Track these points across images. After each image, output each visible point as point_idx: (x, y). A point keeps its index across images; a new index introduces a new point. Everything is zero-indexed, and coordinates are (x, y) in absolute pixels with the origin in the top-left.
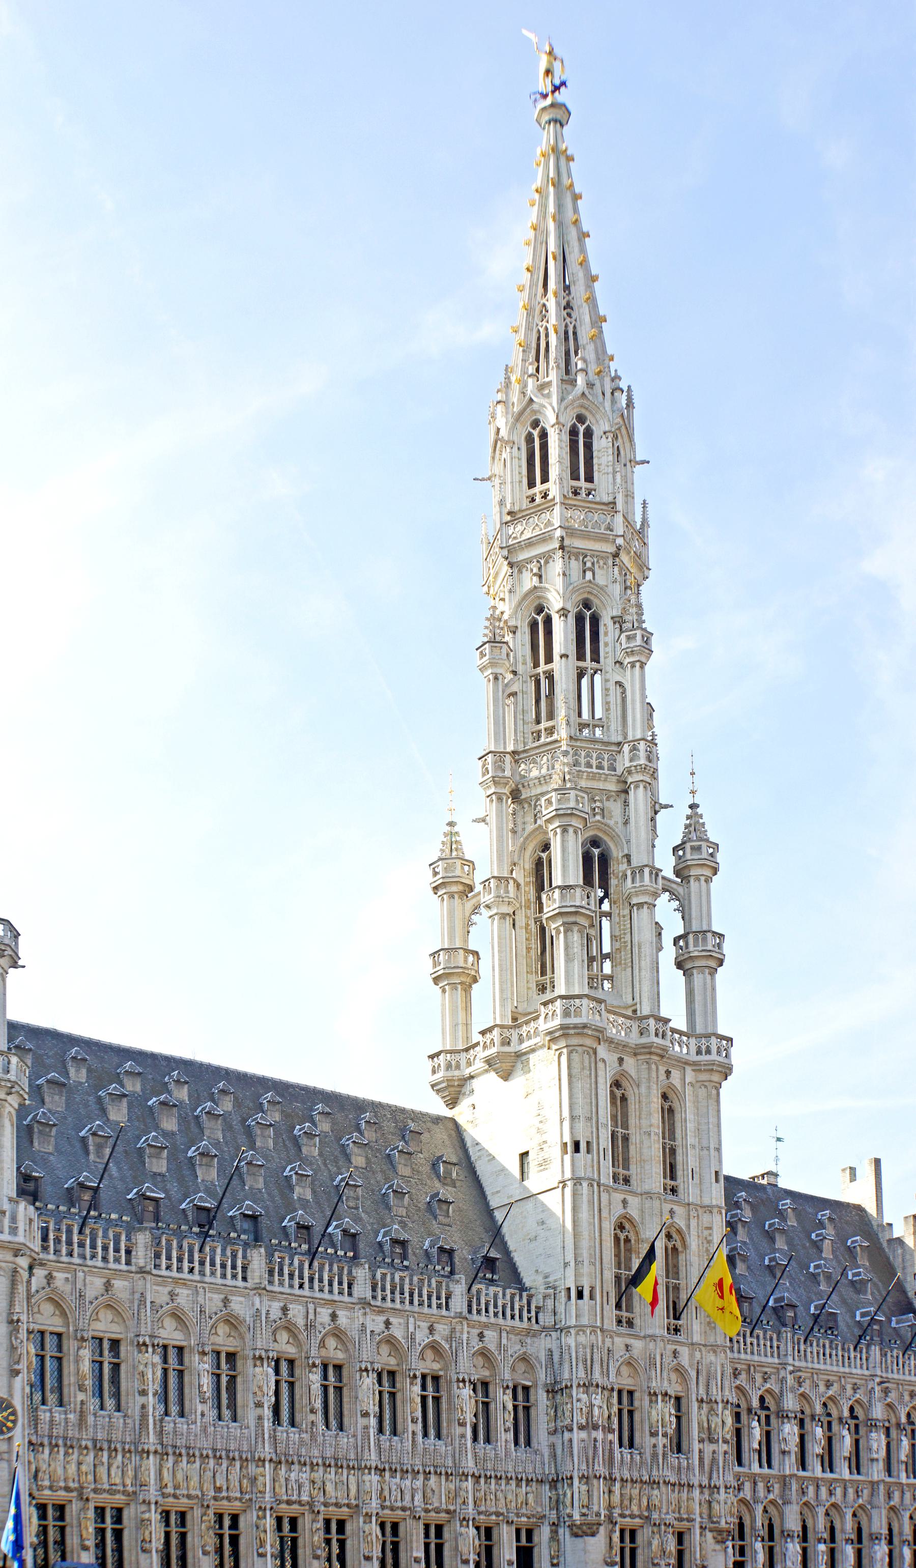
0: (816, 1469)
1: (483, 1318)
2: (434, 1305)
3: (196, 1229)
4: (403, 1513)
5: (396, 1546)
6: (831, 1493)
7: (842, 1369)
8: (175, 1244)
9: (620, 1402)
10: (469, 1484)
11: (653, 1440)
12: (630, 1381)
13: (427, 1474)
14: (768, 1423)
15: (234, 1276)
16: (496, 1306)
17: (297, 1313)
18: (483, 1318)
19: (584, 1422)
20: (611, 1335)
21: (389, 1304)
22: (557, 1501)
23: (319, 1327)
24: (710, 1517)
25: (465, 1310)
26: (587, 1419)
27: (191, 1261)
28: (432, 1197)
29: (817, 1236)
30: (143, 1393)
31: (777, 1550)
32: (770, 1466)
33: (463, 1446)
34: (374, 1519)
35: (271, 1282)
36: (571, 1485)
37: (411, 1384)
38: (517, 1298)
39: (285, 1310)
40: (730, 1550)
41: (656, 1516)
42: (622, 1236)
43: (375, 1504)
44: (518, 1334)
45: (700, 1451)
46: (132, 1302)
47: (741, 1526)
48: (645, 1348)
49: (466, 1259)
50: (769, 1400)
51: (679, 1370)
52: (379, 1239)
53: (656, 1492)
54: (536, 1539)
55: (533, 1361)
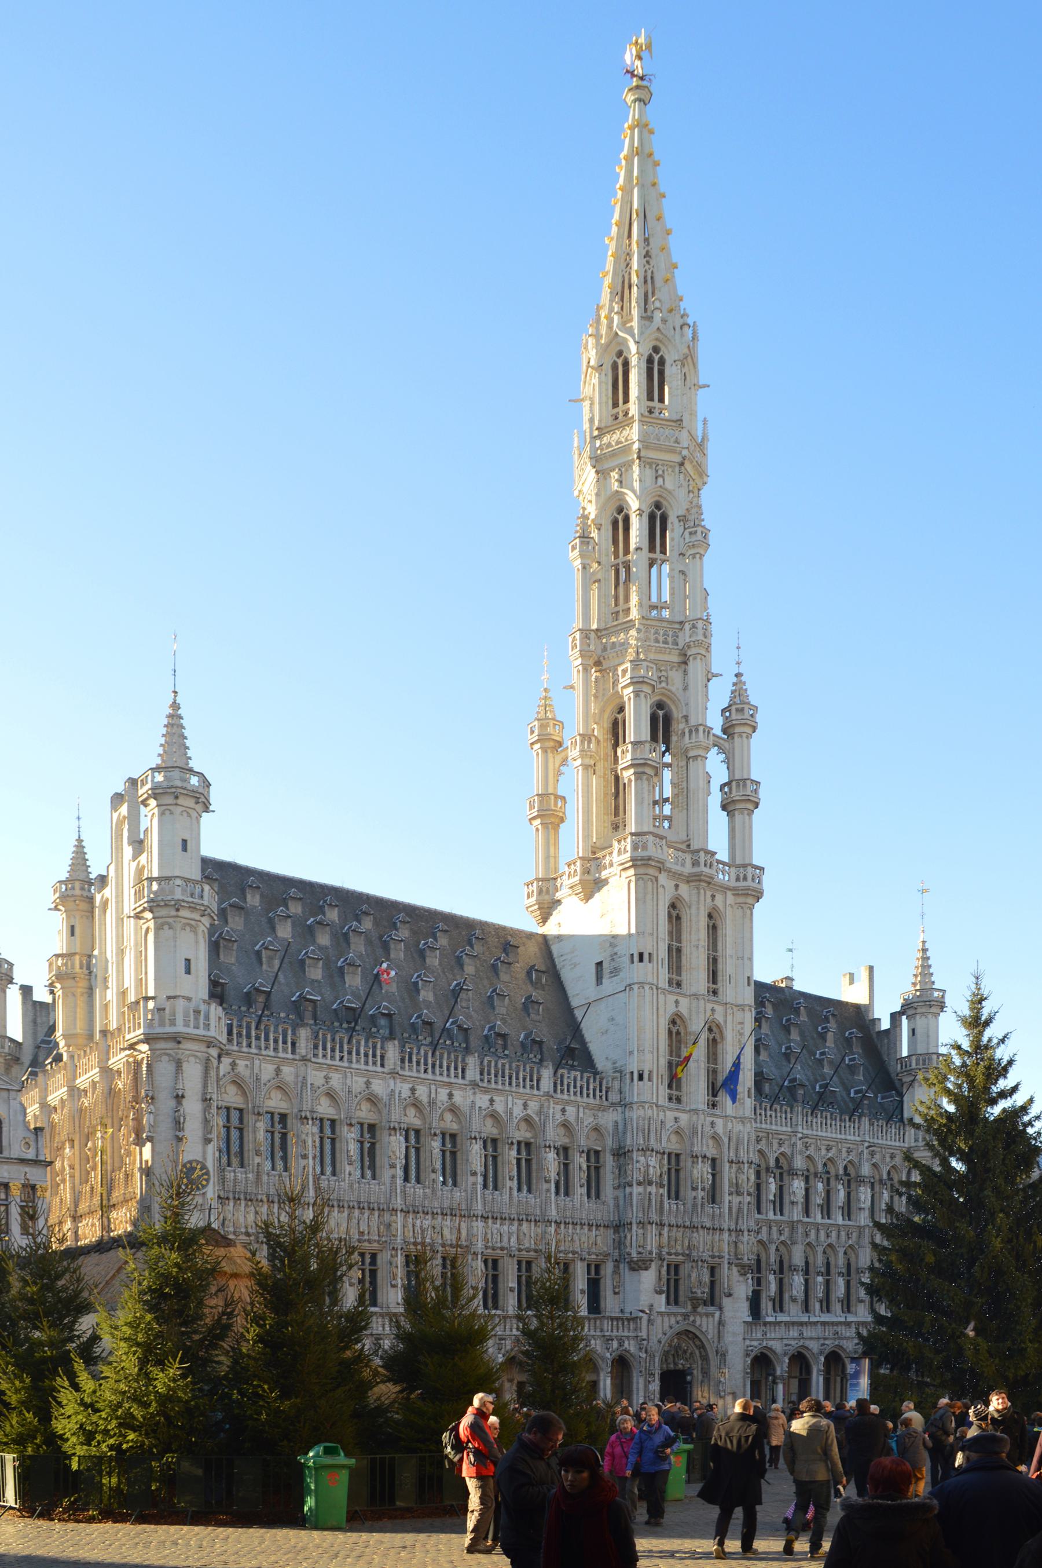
0: (818, 1217)
1: (565, 1097)
2: (528, 1086)
3: (345, 1025)
5: (495, 1278)
6: (828, 1236)
7: (839, 1136)
8: (329, 1037)
9: (669, 1163)
10: (552, 1229)
11: (694, 1193)
12: (678, 1146)
13: (520, 1221)
14: (781, 1180)
15: (374, 1063)
16: (575, 1087)
17: (422, 1092)
18: (565, 1097)
19: (641, 1179)
21: (493, 1086)
22: (619, 1242)
23: (439, 1104)
24: (736, 1254)
25: (552, 1090)
27: (341, 1051)
28: (526, 999)
29: (823, 1028)
30: (305, 1157)
31: (786, 1281)
32: (782, 1214)
33: (548, 1200)
35: (402, 1068)
36: (630, 1230)
37: (510, 1149)
38: (592, 1080)
39: (413, 1090)
40: (750, 1281)
42: (674, 1030)
43: (480, 1246)
45: (730, 1202)
46: (296, 1084)
47: (759, 1261)
48: (690, 1120)
49: (552, 1049)
50: (782, 1160)
51: (715, 1137)
52: (485, 1032)
53: (695, 1235)
54: (602, 1272)
55: (603, 1131)
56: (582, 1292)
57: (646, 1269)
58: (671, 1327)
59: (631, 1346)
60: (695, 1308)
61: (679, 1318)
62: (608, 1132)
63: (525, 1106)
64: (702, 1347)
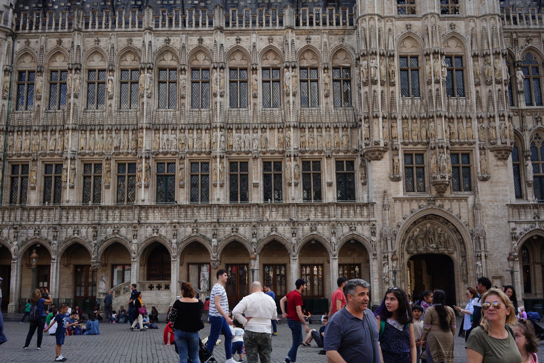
4: (246, 155)
11: (430, 88)
16: (318, 19)
17: (176, 42)
18: (308, 27)
20: (390, 18)
24: (489, 140)
26: (367, 78)
34: (218, 159)
37: (253, 74)
39: (168, 41)
41: (433, 142)
44: (337, 34)
45: (477, 92)
51: (455, 36)
53: (432, 124)
56: (330, 185)
57: (377, 159)
58: (412, 212)
59: (363, 231)
60: (441, 193)
61: (424, 203)
62: (353, 49)
63: (271, 40)
64: (457, 230)
